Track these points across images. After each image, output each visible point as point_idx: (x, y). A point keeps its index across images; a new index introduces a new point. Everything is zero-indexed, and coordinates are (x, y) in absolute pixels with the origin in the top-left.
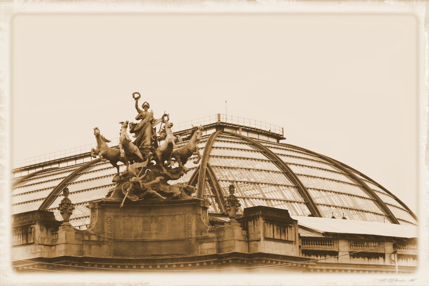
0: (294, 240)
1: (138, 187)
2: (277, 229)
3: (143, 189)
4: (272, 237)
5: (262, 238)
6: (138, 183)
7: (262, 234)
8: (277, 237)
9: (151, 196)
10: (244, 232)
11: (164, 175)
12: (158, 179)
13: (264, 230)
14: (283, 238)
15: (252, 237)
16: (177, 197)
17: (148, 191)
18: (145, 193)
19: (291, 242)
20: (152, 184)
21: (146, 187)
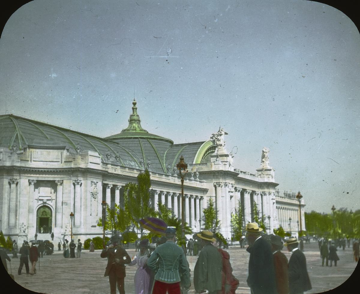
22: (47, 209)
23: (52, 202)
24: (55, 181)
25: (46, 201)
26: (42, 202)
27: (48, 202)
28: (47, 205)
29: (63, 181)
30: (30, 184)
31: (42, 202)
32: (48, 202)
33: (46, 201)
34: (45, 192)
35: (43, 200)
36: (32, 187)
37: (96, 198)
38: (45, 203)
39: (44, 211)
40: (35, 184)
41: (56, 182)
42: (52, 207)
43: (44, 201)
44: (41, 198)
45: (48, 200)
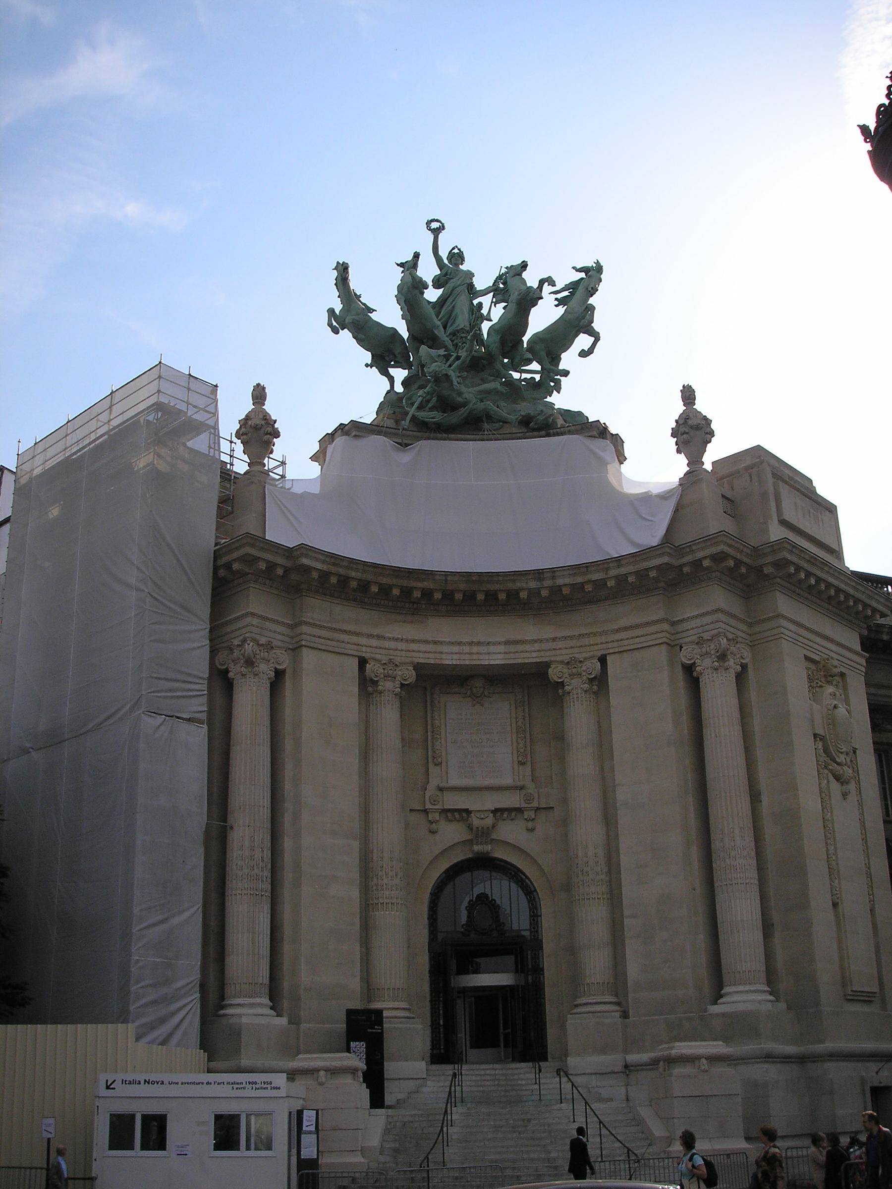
1: (446, 393)
3: (460, 399)
17: (470, 406)
18: (463, 412)
20: (480, 392)
21: (466, 395)
22: (499, 889)
23: (532, 830)
24: (544, 667)
25: (490, 821)
26: (451, 833)
27: (511, 832)
28: (499, 854)
29: (603, 660)
30: (367, 686)
31: (451, 833)
32: (511, 832)
33: (490, 821)
34: (481, 751)
36: (388, 714)
38: (483, 834)
39: (483, 899)
41: (554, 673)
43: (476, 822)
45: (495, 811)
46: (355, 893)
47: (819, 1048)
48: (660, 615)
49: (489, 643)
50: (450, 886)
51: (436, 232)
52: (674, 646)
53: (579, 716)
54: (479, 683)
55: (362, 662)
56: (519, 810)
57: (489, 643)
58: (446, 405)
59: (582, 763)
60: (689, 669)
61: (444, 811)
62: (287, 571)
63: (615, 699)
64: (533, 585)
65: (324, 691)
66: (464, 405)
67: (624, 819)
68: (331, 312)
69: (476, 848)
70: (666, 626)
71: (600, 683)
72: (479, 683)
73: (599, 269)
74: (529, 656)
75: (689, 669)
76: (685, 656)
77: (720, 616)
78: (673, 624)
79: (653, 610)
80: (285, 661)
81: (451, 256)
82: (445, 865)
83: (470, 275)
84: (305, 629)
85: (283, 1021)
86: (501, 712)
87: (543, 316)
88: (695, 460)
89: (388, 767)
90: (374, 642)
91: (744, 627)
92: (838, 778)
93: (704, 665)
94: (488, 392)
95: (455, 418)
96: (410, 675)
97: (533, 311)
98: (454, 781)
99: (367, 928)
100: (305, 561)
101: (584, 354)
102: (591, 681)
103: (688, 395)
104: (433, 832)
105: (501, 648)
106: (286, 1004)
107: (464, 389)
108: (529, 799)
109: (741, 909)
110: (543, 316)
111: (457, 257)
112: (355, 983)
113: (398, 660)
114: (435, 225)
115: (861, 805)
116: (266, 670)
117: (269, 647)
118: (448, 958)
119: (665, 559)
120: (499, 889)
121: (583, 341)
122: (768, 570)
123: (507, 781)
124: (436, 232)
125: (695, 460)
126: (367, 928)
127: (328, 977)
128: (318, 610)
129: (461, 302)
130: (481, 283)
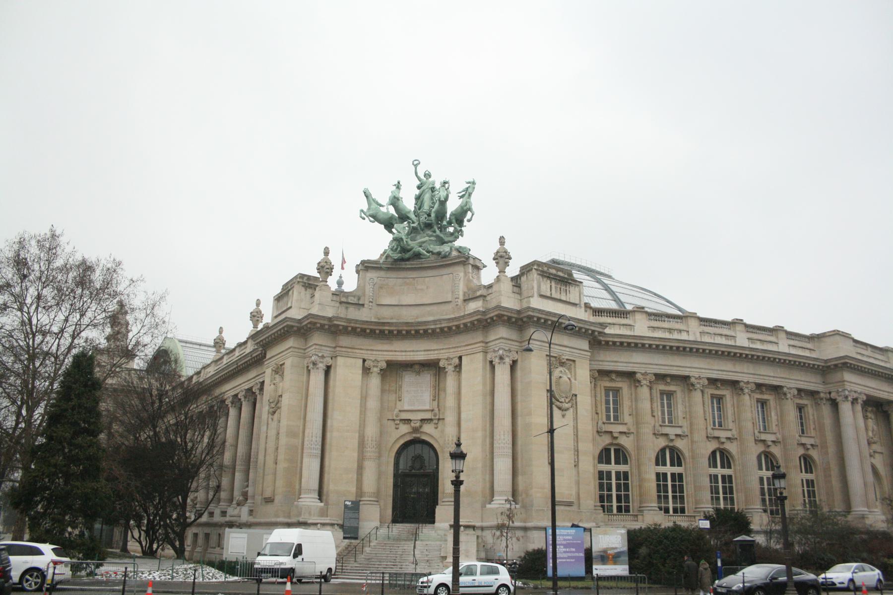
0: (577, 302)
2: (556, 288)
4: (549, 295)
5: (536, 295)
6: (402, 239)
7: (535, 289)
8: (555, 295)
9: (418, 256)
10: (516, 289)
11: (437, 236)
12: (427, 238)
13: (539, 287)
14: (563, 298)
15: (525, 294)
16: (445, 257)
18: (411, 253)
19: (575, 305)
24: (439, 360)
25: (418, 425)
26: (404, 429)
27: (428, 428)
29: (460, 358)
30: (366, 371)
31: (404, 429)
32: (428, 428)
35: (408, 421)
36: (375, 381)
37: (567, 410)
38: (416, 430)
40: (384, 373)
41: (441, 364)
42: (437, 441)
44: (404, 416)
45: (423, 420)
46: (356, 455)
47: (529, 524)
48: (480, 339)
49: (417, 351)
50: (405, 452)
51: (416, 166)
52: (485, 352)
53: (450, 381)
54: (417, 367)
55: (364, 361)
56: (431, 420)
57: (417, 351)
58: (404, 250)
59: (450, 401)
60: (491, 362)
61: (401, 420)
62: (330, 326)
63: (464, 375)
64: (433, 327)
65: (348, 371)
66: (411, 250)
67: (464, 425)
68: (362, 211)
69: (414, 435)
70: (483, 345)
71: (459, 367)
72: (417, 367)
73: (474, 183)
74: (432, 356)
75: (491, 362)
76: (489, 357)
77: (501, 340)
78: (487, 343)
79: (478, 337)
80: (329, 361)
81: (425, 176)
82: (402, 442)
83: (434, 183)
84: (338, 349)
85: (322, 504)
86: (427, 378)
87: (452, 206)
88: (502, 271)
89: (373, 404)
90: (369, 352)
91: (517, 344)
92: (560, 408)
93: (497, 360)
94: (424, 242)
95: (407, 256)
96: (384, 365)
97: (448, 203)
98: (406, 408)
99: (360, 468)
100: (335, 322)
101: (469, 221)
102: (456, 367)
103: (502, 241)
104: (397, 428)
105: (423, 353)
106: (324, 498)
107: (410, 242)
108: (435, 415)
109: (503, 465)
110: (452, 206)
111: (428, 175)
112: (353, 489)
113: (379, 359)
114: (416, 163)
115: (576, 419)
116: (322, 366)
117: (323, 357)
118: (402, 481)
119: (479, 317)
120: (426, 453)
121: (469, 214)
122: (525, 320)
123: (427, 407)
124: (416, 166)
125: (502, 271)
126: (360, 468)
127: (342, 486)
128: (345, 341)
129: (427, 197)
130: (438, 186)
